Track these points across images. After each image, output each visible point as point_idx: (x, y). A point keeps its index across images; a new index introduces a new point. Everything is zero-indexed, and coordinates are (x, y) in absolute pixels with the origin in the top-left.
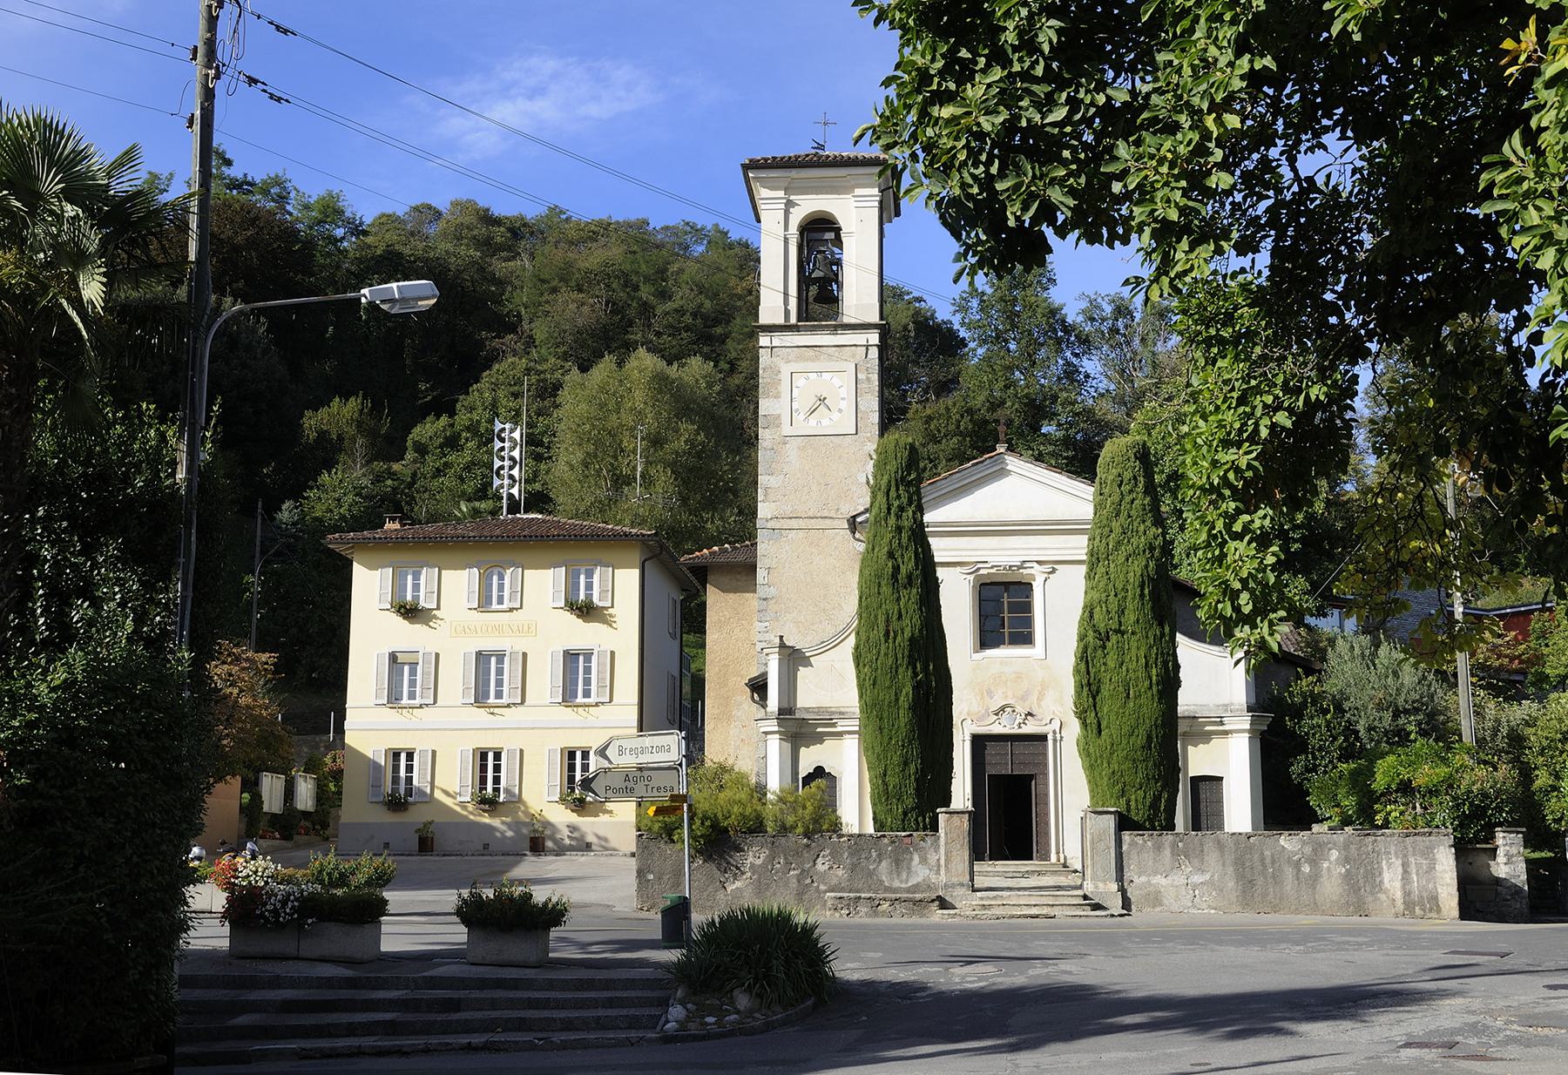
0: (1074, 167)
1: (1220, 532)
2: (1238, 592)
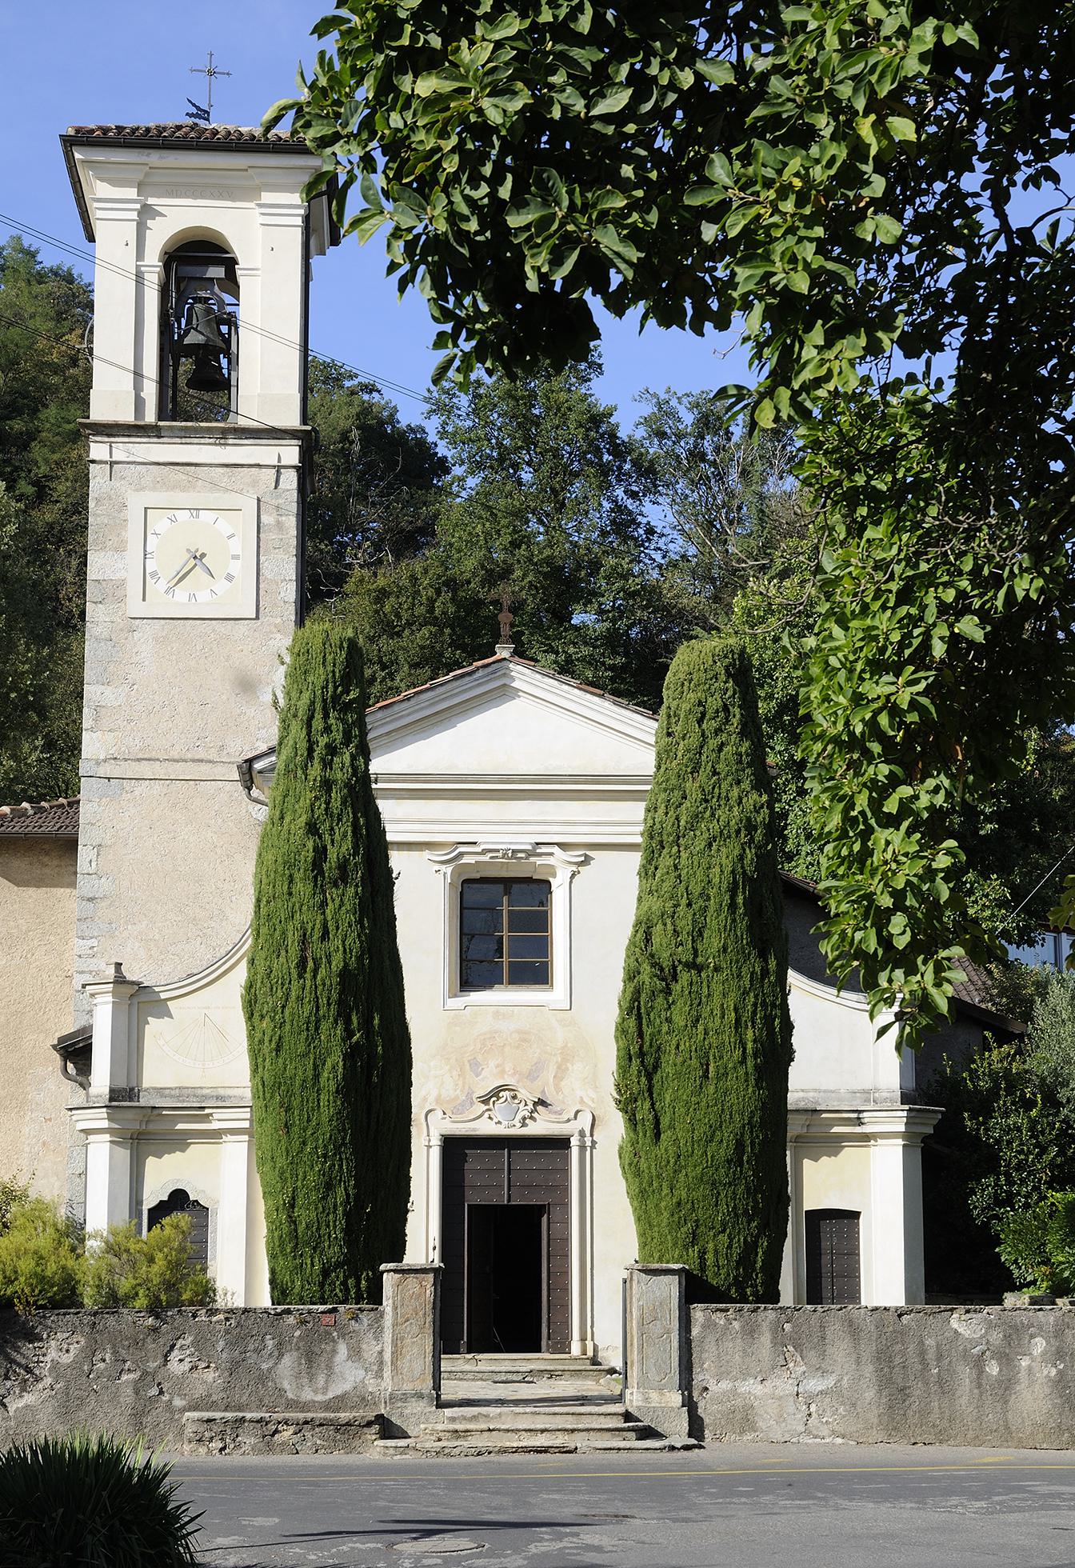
0: (639, 193)
1: (862, 813)
2: (889, 913)
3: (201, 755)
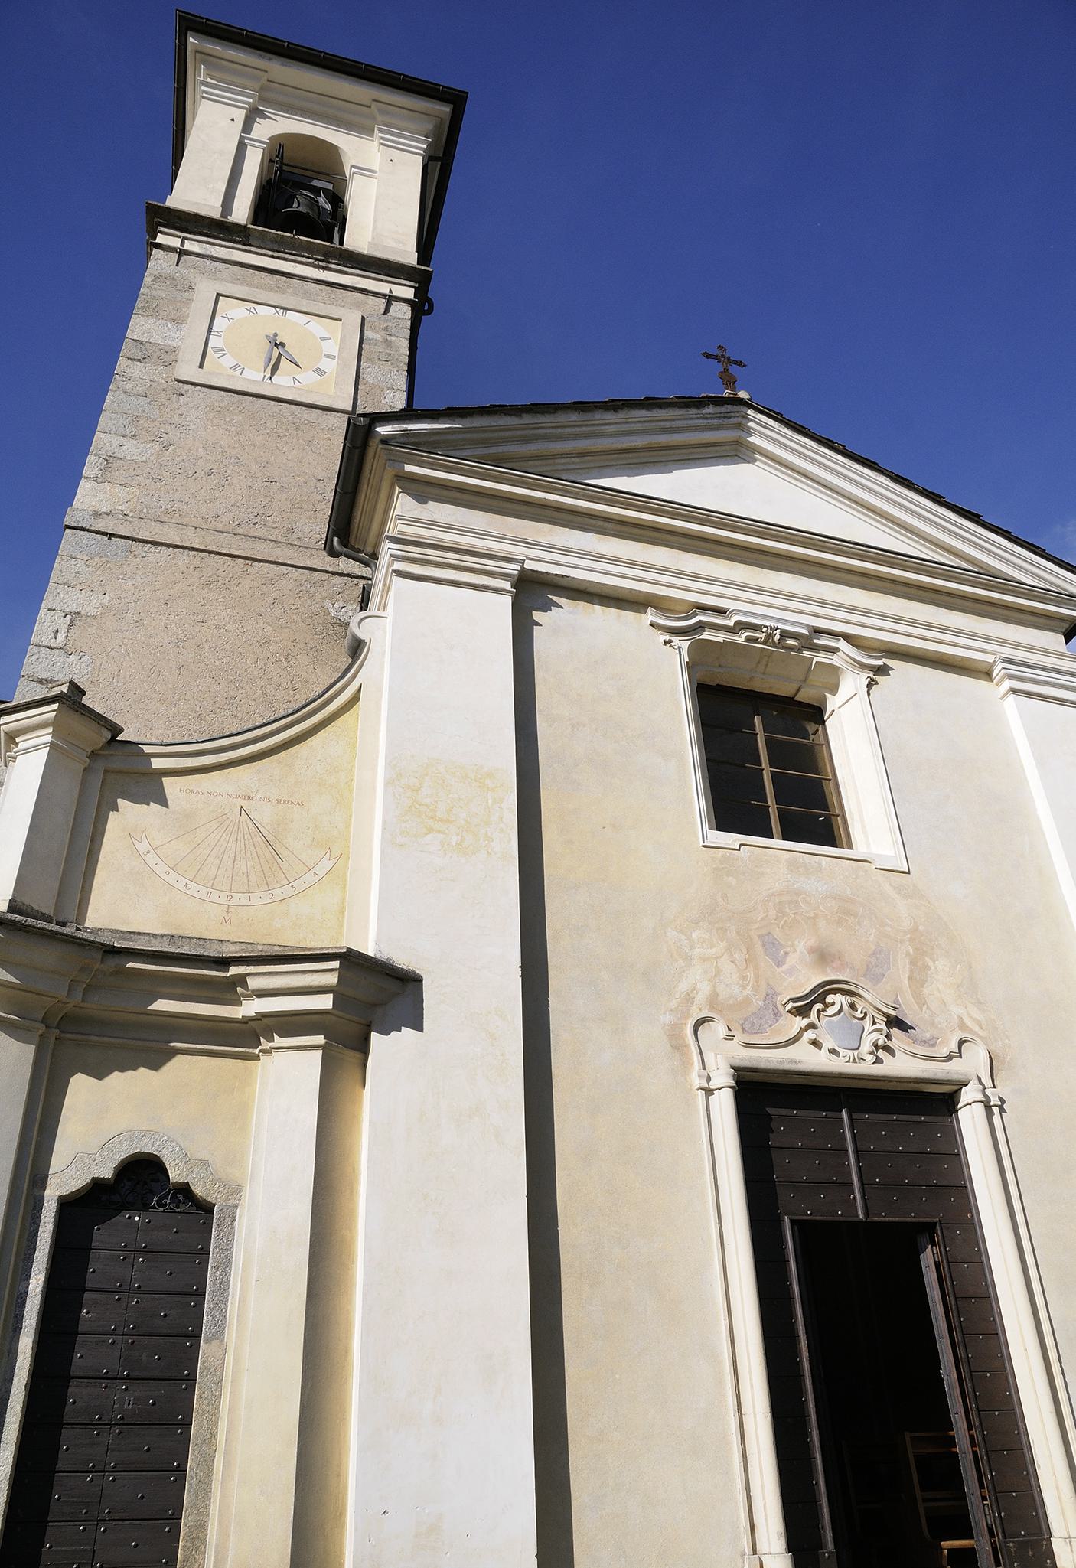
3: (259, 531)
